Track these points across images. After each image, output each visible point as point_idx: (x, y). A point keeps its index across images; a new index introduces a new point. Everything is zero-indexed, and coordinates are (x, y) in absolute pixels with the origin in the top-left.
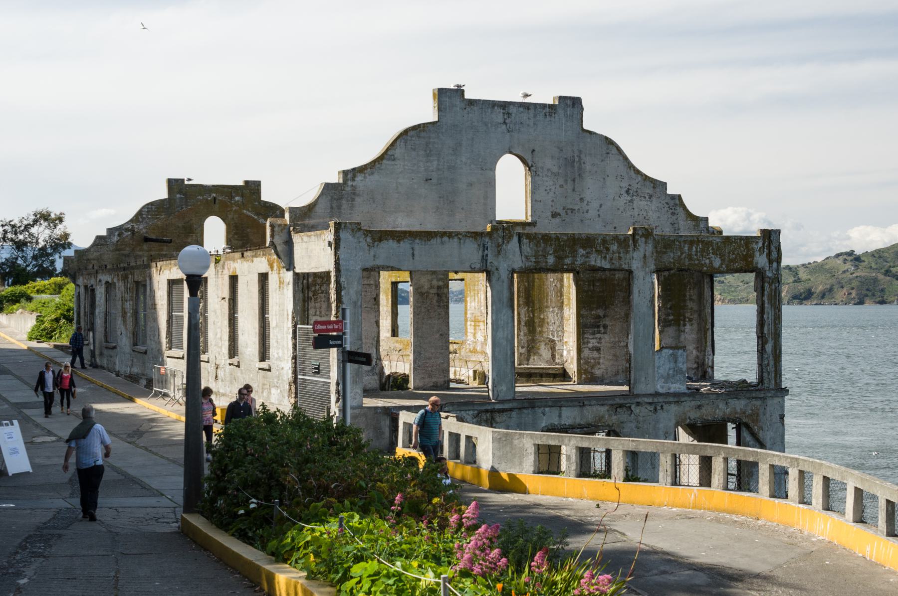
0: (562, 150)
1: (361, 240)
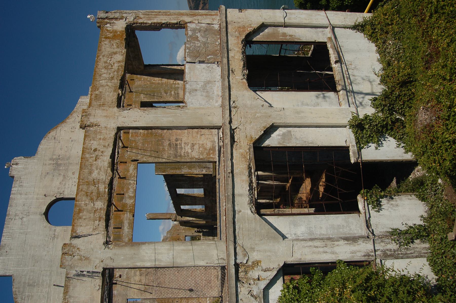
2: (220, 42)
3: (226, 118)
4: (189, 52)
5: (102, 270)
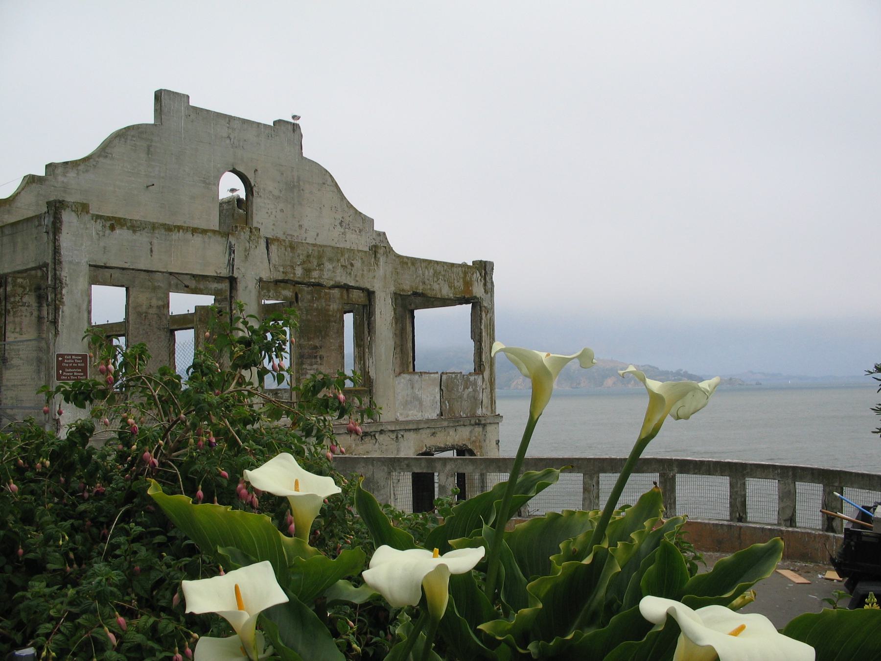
0: (282, 174)
1: (88, 226)
2: (464, 417)
3: (387, 426)
4: (452, 378)
5: (236, 277)
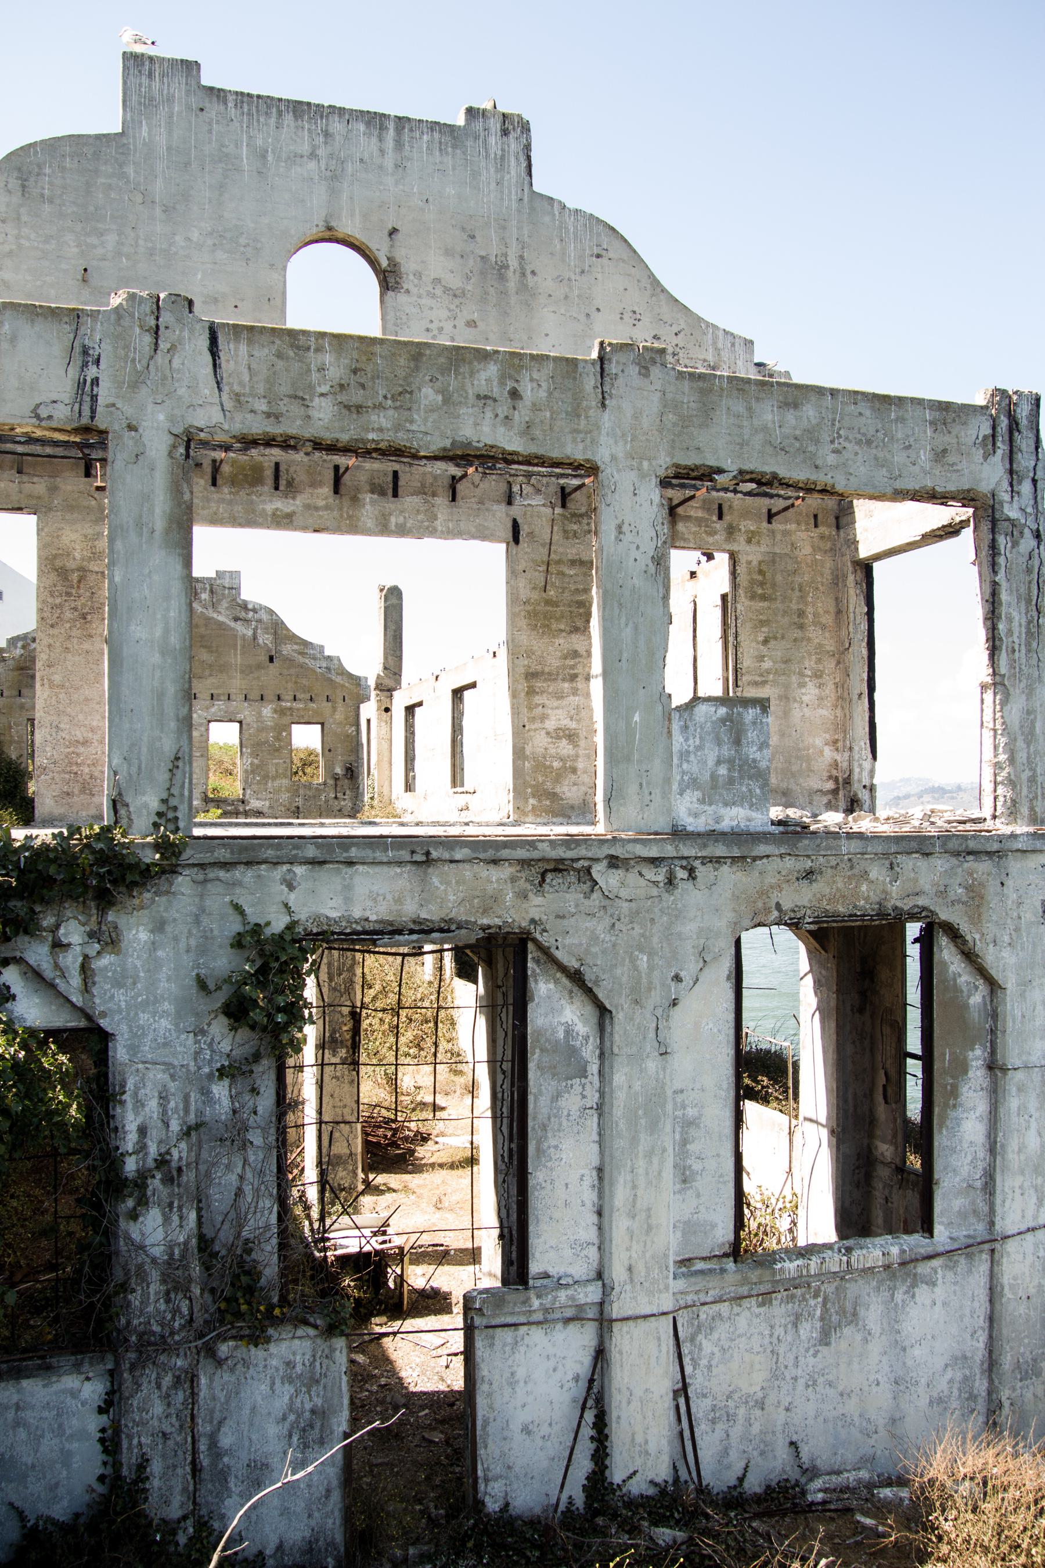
0: (473, 237)
